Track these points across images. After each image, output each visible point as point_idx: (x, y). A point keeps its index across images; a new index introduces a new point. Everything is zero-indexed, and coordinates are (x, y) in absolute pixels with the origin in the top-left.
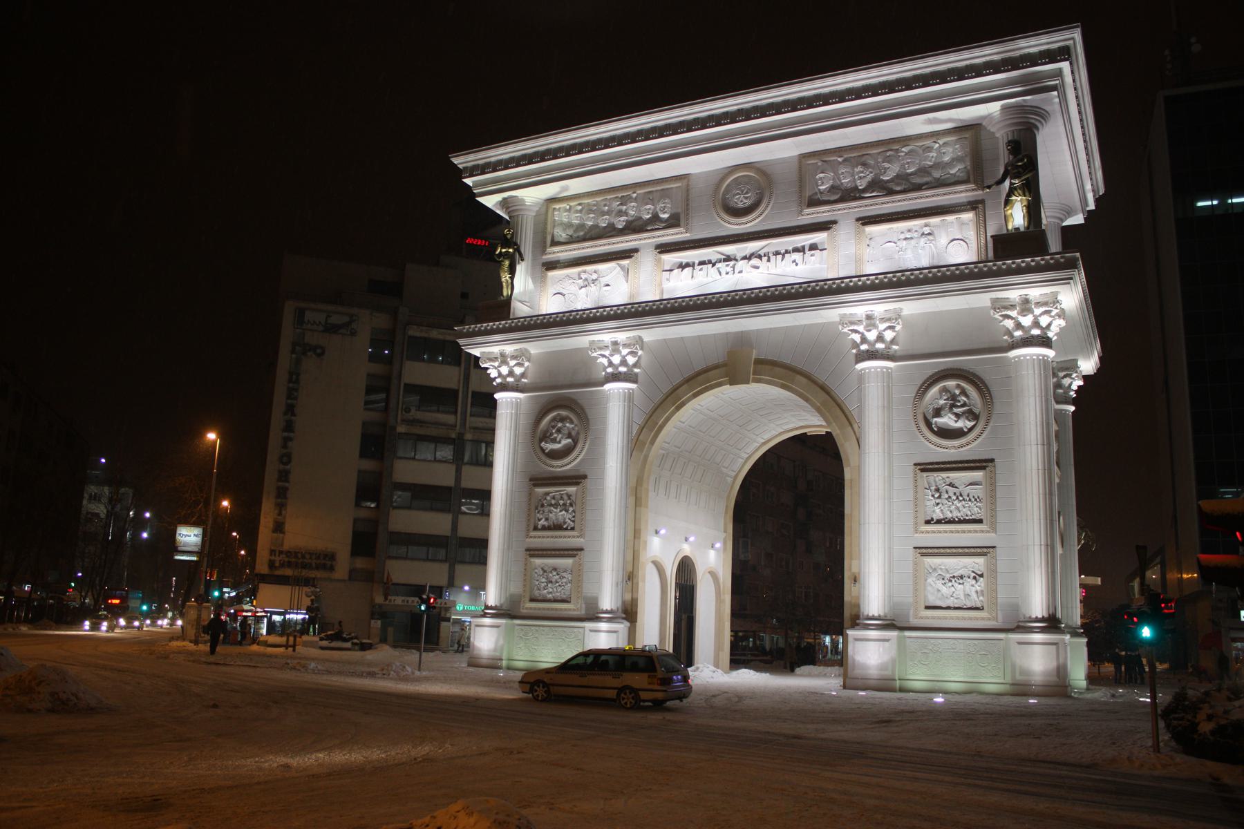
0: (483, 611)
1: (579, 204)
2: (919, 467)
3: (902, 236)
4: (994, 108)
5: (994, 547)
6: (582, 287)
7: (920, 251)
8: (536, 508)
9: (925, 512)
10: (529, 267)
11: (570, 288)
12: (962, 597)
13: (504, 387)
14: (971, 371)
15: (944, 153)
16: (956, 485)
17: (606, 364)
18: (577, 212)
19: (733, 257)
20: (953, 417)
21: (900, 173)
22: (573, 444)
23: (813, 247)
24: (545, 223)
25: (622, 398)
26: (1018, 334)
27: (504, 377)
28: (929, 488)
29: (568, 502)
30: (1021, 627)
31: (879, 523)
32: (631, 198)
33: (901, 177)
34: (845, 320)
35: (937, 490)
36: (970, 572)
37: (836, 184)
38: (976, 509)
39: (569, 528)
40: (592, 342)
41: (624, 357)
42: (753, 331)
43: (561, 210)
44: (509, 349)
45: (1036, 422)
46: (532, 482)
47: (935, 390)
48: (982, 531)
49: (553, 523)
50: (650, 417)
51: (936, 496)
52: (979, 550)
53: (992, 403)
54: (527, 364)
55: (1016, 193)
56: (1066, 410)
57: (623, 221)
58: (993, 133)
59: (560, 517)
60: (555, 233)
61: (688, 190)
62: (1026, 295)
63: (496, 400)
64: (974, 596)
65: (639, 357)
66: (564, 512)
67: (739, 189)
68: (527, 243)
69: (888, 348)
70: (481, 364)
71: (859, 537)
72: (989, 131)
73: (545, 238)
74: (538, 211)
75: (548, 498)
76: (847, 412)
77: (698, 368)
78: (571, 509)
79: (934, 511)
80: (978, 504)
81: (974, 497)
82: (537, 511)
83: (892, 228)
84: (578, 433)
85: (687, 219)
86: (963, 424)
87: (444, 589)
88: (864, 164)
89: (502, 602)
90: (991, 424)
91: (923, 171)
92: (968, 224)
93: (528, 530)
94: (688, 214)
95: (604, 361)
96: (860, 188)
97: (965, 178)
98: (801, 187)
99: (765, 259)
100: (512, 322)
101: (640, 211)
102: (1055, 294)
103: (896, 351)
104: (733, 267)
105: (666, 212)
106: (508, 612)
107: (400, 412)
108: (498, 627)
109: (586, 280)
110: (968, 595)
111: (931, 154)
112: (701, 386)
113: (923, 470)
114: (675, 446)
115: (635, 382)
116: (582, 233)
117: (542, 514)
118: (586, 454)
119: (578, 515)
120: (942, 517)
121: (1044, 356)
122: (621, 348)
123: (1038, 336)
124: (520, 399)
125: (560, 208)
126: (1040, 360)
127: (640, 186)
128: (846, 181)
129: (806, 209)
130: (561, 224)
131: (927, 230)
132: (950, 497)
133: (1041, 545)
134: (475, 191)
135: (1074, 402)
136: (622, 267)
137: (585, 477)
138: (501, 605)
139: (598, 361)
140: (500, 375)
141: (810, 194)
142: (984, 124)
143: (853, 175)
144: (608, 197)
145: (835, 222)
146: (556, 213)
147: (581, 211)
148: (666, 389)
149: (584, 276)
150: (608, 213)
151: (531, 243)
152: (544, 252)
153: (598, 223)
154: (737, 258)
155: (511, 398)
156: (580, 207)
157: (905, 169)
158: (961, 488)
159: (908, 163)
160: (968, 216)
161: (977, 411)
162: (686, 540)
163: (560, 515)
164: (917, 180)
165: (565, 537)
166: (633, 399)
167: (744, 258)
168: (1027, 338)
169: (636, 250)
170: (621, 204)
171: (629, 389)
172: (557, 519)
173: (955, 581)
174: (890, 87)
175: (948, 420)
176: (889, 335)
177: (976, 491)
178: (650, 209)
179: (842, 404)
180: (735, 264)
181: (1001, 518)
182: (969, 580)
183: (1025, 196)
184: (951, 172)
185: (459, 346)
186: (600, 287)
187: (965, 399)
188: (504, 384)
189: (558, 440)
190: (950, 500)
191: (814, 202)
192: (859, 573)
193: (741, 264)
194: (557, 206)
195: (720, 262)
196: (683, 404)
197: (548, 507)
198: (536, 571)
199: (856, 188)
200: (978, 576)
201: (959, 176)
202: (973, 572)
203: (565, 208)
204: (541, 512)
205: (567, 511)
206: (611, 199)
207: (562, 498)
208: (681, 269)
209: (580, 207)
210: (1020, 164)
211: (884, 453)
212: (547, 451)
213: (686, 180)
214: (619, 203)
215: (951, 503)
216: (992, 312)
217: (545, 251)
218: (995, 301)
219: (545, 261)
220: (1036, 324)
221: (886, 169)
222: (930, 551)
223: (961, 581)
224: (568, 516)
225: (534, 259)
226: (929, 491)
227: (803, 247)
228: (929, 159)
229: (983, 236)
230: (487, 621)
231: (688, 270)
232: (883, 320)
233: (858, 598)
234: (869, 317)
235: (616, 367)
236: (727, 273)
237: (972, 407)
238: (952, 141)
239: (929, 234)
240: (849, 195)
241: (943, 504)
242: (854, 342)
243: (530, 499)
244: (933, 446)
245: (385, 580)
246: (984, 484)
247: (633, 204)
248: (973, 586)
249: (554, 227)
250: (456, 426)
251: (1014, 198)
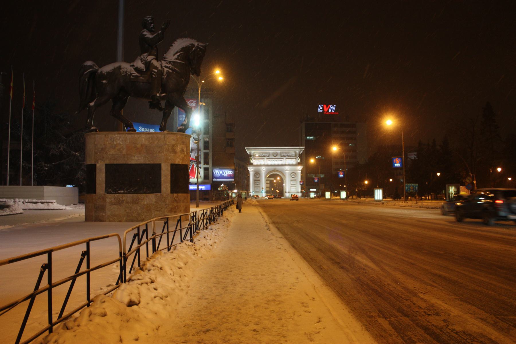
11: (258, 162)
13: (251, 171)
30: (298, 192)
33: (289, 155)
86: (294, 177)
128: (284, 155)
152: (254, 157)
160: (295, 160)
163: (258, 184)
175: (293, 176)
191: (282, 156)
200: (295, 189)
240: (285, 156)
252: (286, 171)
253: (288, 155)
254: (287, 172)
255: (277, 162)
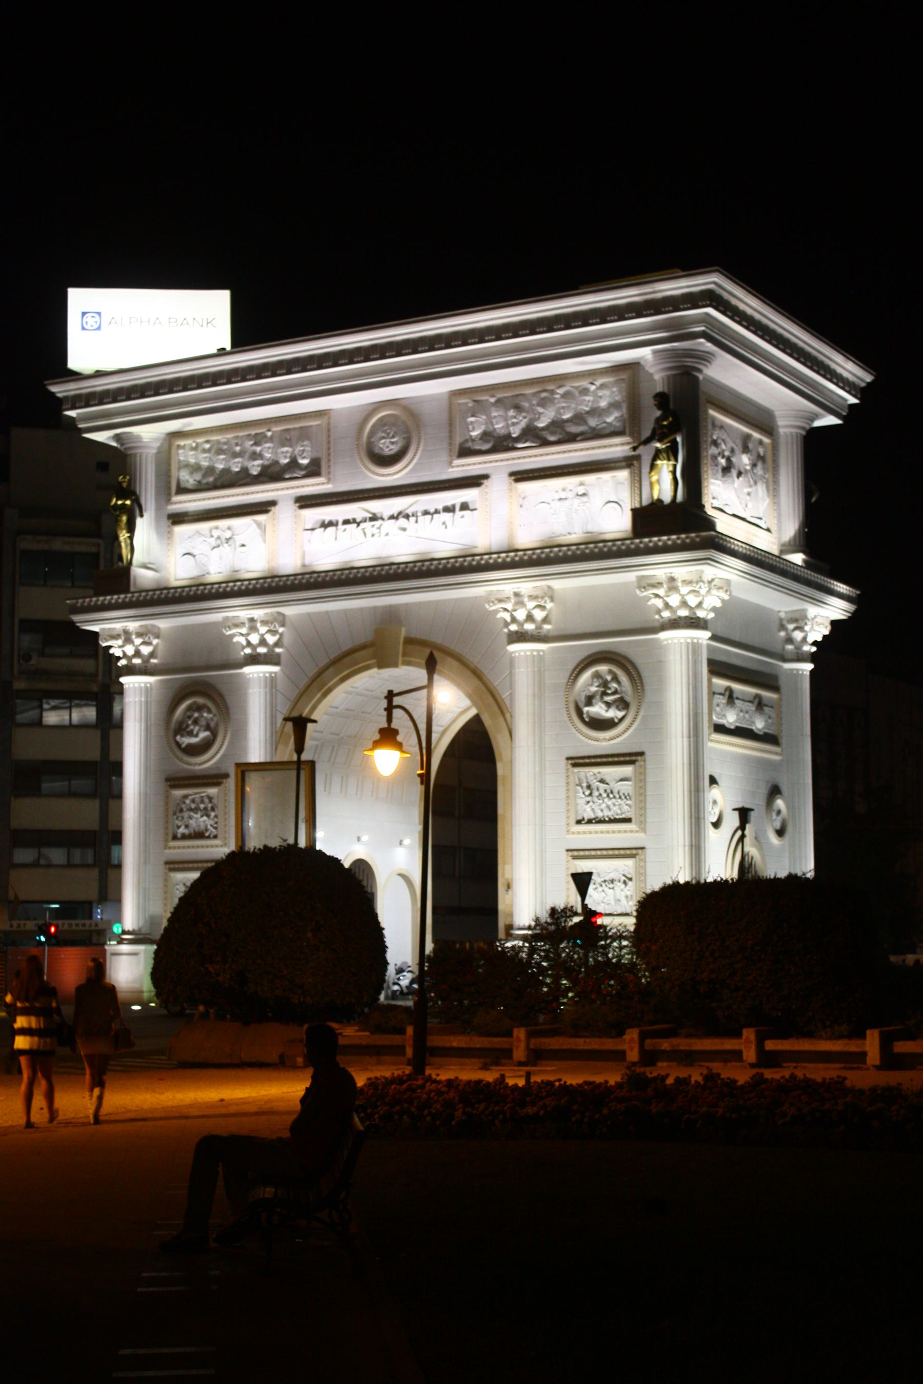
0: (119, 936)
1: (208, 442)
2: (570, 762)
3: (557, 496)
4: (645, 353)
5: (643, 848)
6: (214, 548)
7: (574, 514)
8: (175, 814)
9: (576, 812)
10: (153, 520)
12: (613, 902)
13: (131, 670)
14: (623, 654)
15: (601, 397)
16: (608, 781)
17: (244, 643)
18: (205, 451)
19: (379, 515)
20: (603, 706)
21: (555, 419)
22: (212, 738)
23: (465, 507)
24: (169, 465)
25: (262, 684)
26: (666, 614)
27: (129, 659)
28: (580, 785)
29: (210, 805)
31: (529, 825)
32: (266, 436)
33: (556, 425)
34: (488, 599)
35: (589, 787)
36: (621, 876)
37: (488, 430)
38: (626, 808)
39: (212, 836)
40: (227, 618)
41: (262, 635)
42: (402, 605)
43: (187, 448)
44: (133, 626)
45: (682, 713)
46: (168, 784)
47: (587, 675)
48: (631, 831)
49: (194, 831)
50: (298, 701)
51: (587, 792)
52: (628, 852)
53: (643, 690)
54: (155, 642)
55: (661, 457)
56: (803, 670)
57: (258, 466)
58: (651, 375)
59: (202, 824)
60: (182, 478)
61: (329, 430)
62: (671, 573)
63: (122, 685)
64: (624, 901)
65: (281, 635)
66: (205, 818)
67: (384, 431)
68: (149, 496)
69: (539, 627)
70: (101, 643)
71: (511, 840)
72: (647, 372)
73: (169, 483)
74: (159, 448)
75: (188, 801)
76: (500, 700)
77: (346, 647)
78: (213, 814)
79: (585, 810)
80: (629, 802)
81: (624, 794)
82: (175, 817)
83: (546, 486)
84: (217, 725)
85: (329, 467)
86: (613, 713)
87: (94, 905)
88: (518, 408)
89: (141, 924)
90: (641, 713)
91: (579, 418)
92: (622, 483)
93: (166, 841)
94: (329, 461)
95: (243, 641)
96: (514, 436)
97: (621, 429)
98: (451, 431)
99: (412, 519)
100: (133, 596)
101: (276, 453)
102: (702, 571)
103: (549, 630)
104: (379, 528)
105: (304, 458)
106: (147, 936)
107: (16, 658)
108: (135, 954)
109: (219, 538)
110: (619, 900)
111: (587, 398)
112: (348, 668)
113: (575, 765)
114: (332, 734)
115: (277, 663)
116: (211, 479)
117: (181, 820)
118: (228, 747)
119: (221, 820)
120: (593, 816)
121: (692, 638)
122: (259, 625)
123: (686, 617)
124: (151, 684)
125: (185, 445)
126: (688, 643)
127: (276, 422)
128: (499, 426)
129: (455, 460)
130: (187, 465)
131: (581, 490)
132: (600, 795)
133: (685, 846)
134: (81, 426)
135: (813, 658)
136: (259, 525)
137: (226, 776)
138: (140, 929)
139: (236, 639)
140: (124, 653)
141: (458, 440)
142: (642, 363)
143: (506, 419)
144: (241, 434)
145: (486, 477)
146: (181, 451)
147: (209, 451)
148: (312, 671)
149: (216, 533)
150: (239, 455)
151: (153, 488)
152: (168, 501)
153: (230, 467)
154: (384, 517)
155: (139, 683)
156: (207, 446)
157: (561, 414)
158: (612, 784)
159: (563, 408)
161: (628, 699)
162: (359, 839)
163: (200, 821)
164: (573, 429)
165: (207, 847)
166: (276, 683)
167: (392, 517)
168: (675, 620)
169: (273, 503)
170: (256, 444)
171: (271, 673)
172: (199, 826)
173: (606, 886)
174: (532, 327)
175: (598, 710)
176: (539, 615)
177: (626, 787)
178: (287, 452)
179: (495, 692)
180: (381, 525)
181: (651, 817)
182: (619, 884)
183: (669, 460)
184: (610, 419)
185: (73, 623)
186: (235, 548)
187: (614, 685)
188: (130, 667)
189: (195, 732)
190: (600, 798)
191: (465, 452)
192: (512, 880)
193: (389, 525)
194: (182, 443)
195: (365, 521)
196: (329, 691)
197: (188, 812)
198: (178, 887)
199: (508, 436)
200: (627, 880)
201: (615, 426)
202: (624, 875)
203: (190, 445)
204: (180, 818)
205: (208, 816)
206: (243, 436)
207: (202, 802)
208: (323, 529)
209: (207, 446)
210: (665, 423)
211: (535, 746)
212: (183, 746)
213: (326, 417)
214: (251, 442)
215: (601, 801)
216: (638, 592)
217: (170, 500)
218: (640, 579)
219: (171, 512)
220: (684, 604)
221: (540, 414)
222: (581, 853)
223: (611, 886)
224: (209, 822)
225: (158, 509)
226: (579, 788)
227: (454, 506)
228: (586, 403)
229: (637, 498)
230: (125, 948)
231: (331, 530)
232: (532, 597)
233: (511, 906)
234: (517, 595)
235: (254, 647)
236: (373, 535)
237: (623, 695)
238: (610, 382)
239: (584, 495)
241: (593, 802)
242: (506, 621)
243: (167, 804)
244: (587, 740)
245: (11, 896)
246: (633, 779)
247: (268, 445)
248: (622, 890)
249: (179, 469)
250: (97, 675)
251: (659, 462)
252: (520, 637)
253: (541, 425)
254: (514, 648)
255: (410, 524)
